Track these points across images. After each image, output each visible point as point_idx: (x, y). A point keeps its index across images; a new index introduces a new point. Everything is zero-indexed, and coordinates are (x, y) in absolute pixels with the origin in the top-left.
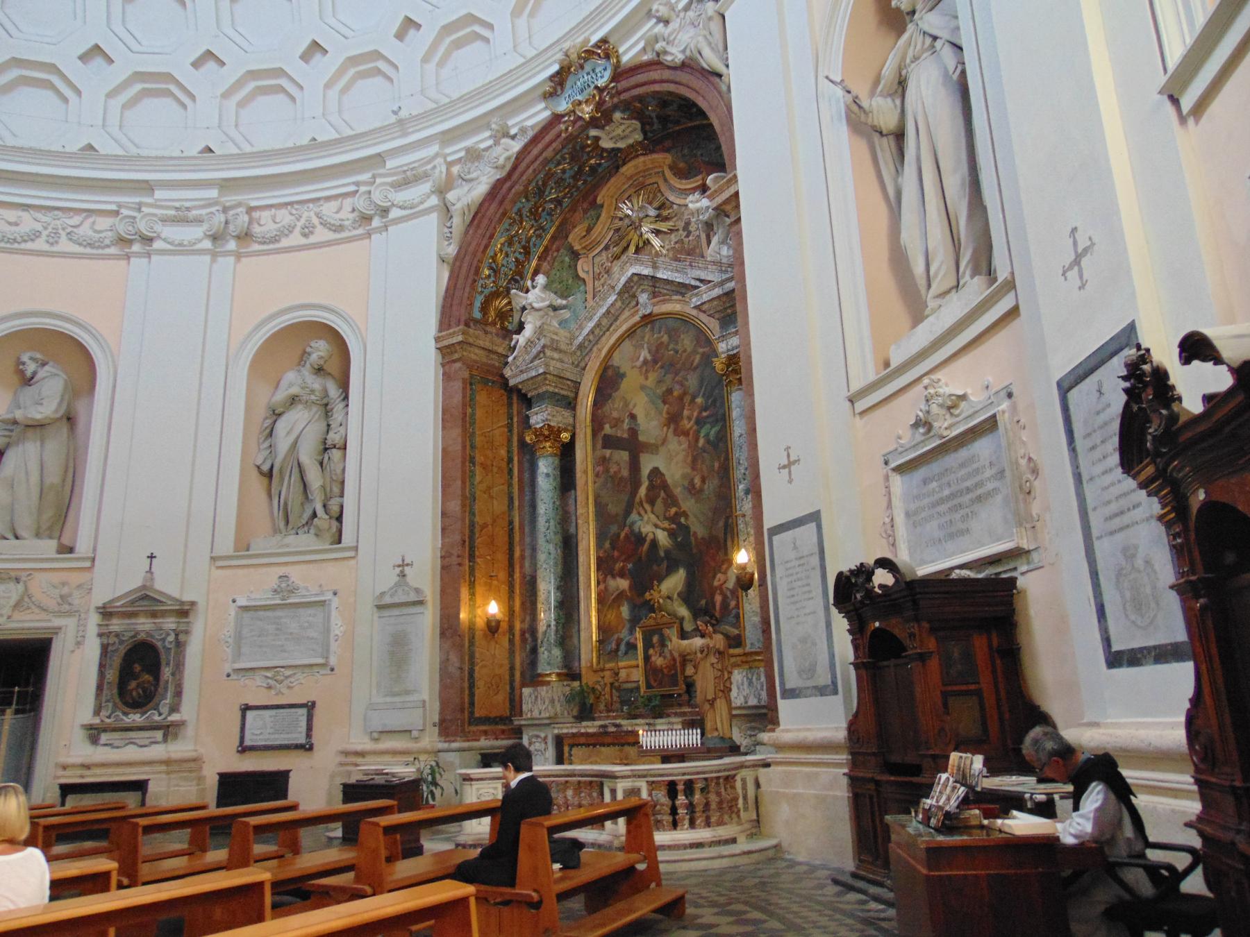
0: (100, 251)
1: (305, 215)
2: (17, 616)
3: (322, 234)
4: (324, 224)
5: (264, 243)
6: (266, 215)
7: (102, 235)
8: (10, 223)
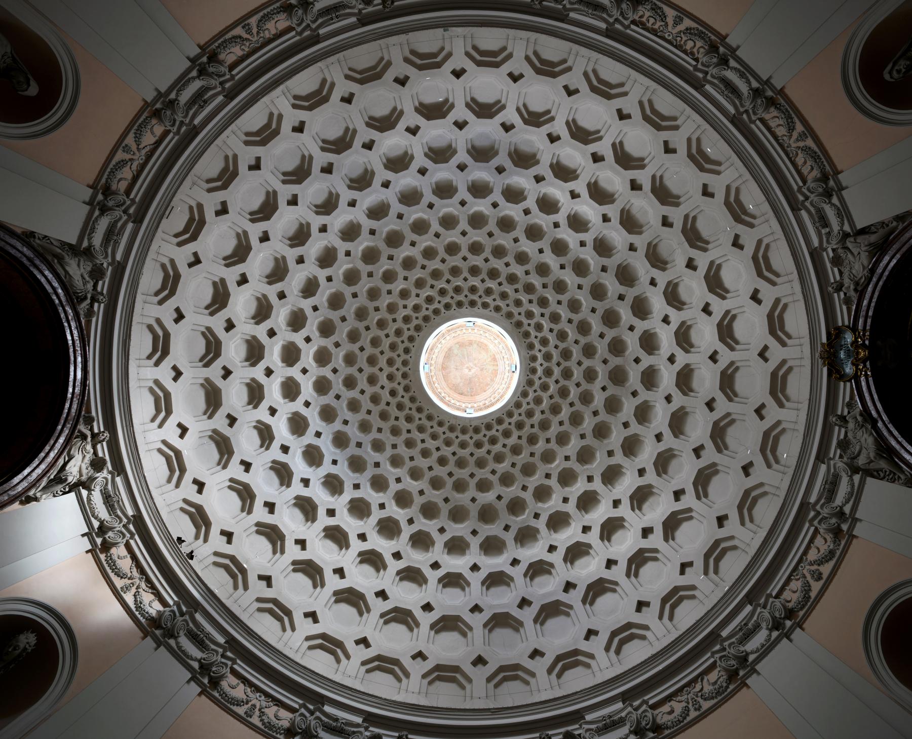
1: (805, 572)
3: (826, 569)
4: (820, 562)
5: (804, 606)
6: (787, 595)
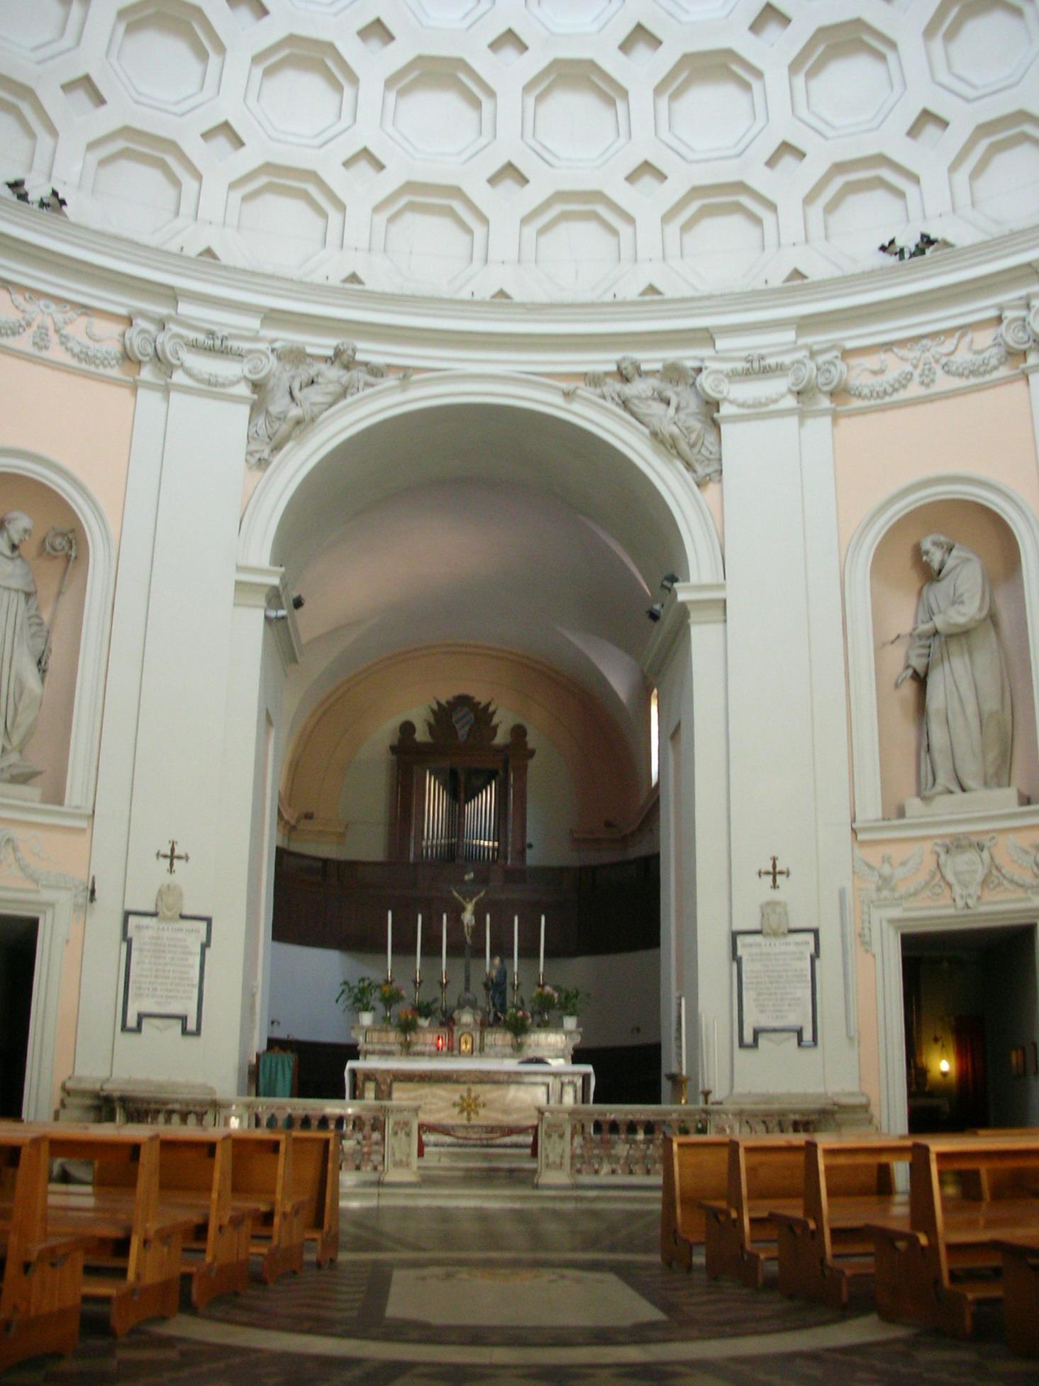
0: (988, 378)
2: (988, 896)
7: (986, 354)
8: (874, 373)
